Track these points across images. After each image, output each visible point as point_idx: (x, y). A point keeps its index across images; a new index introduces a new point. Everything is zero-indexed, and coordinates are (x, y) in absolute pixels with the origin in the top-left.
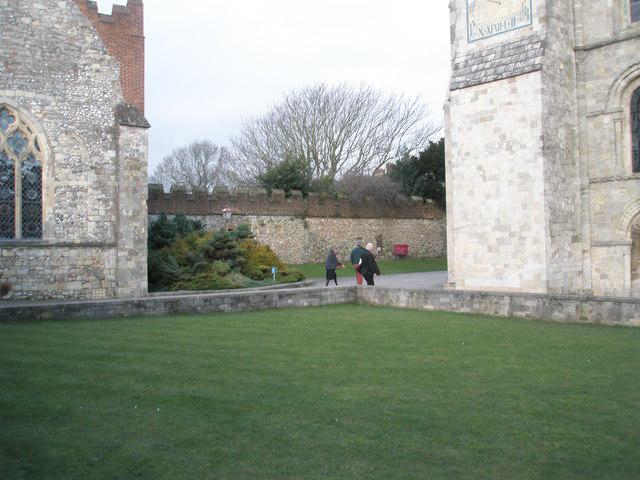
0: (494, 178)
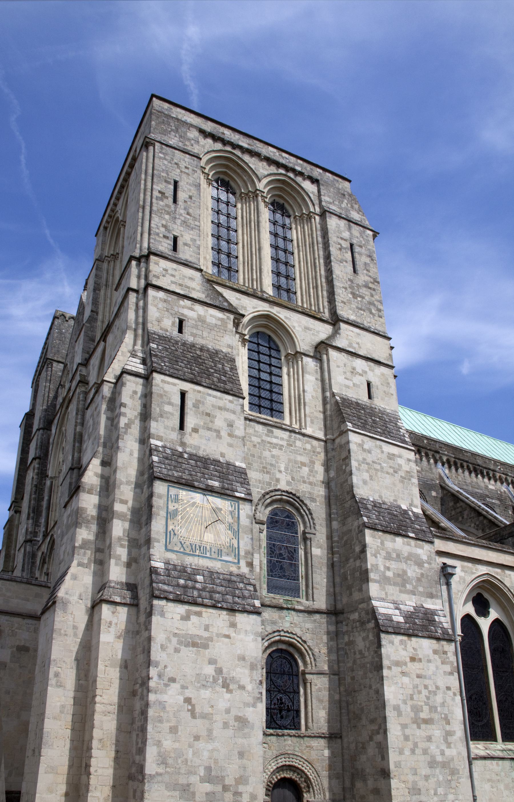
0: (205, 716)
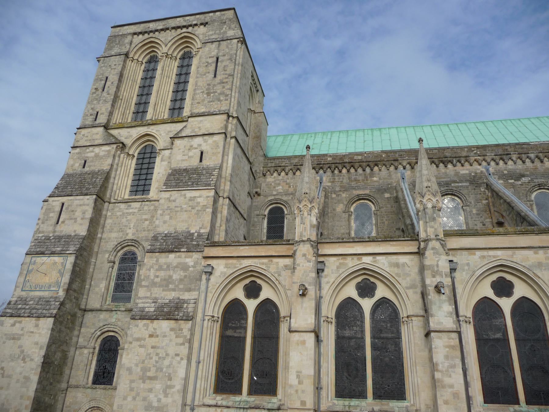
0: (9, 377)
